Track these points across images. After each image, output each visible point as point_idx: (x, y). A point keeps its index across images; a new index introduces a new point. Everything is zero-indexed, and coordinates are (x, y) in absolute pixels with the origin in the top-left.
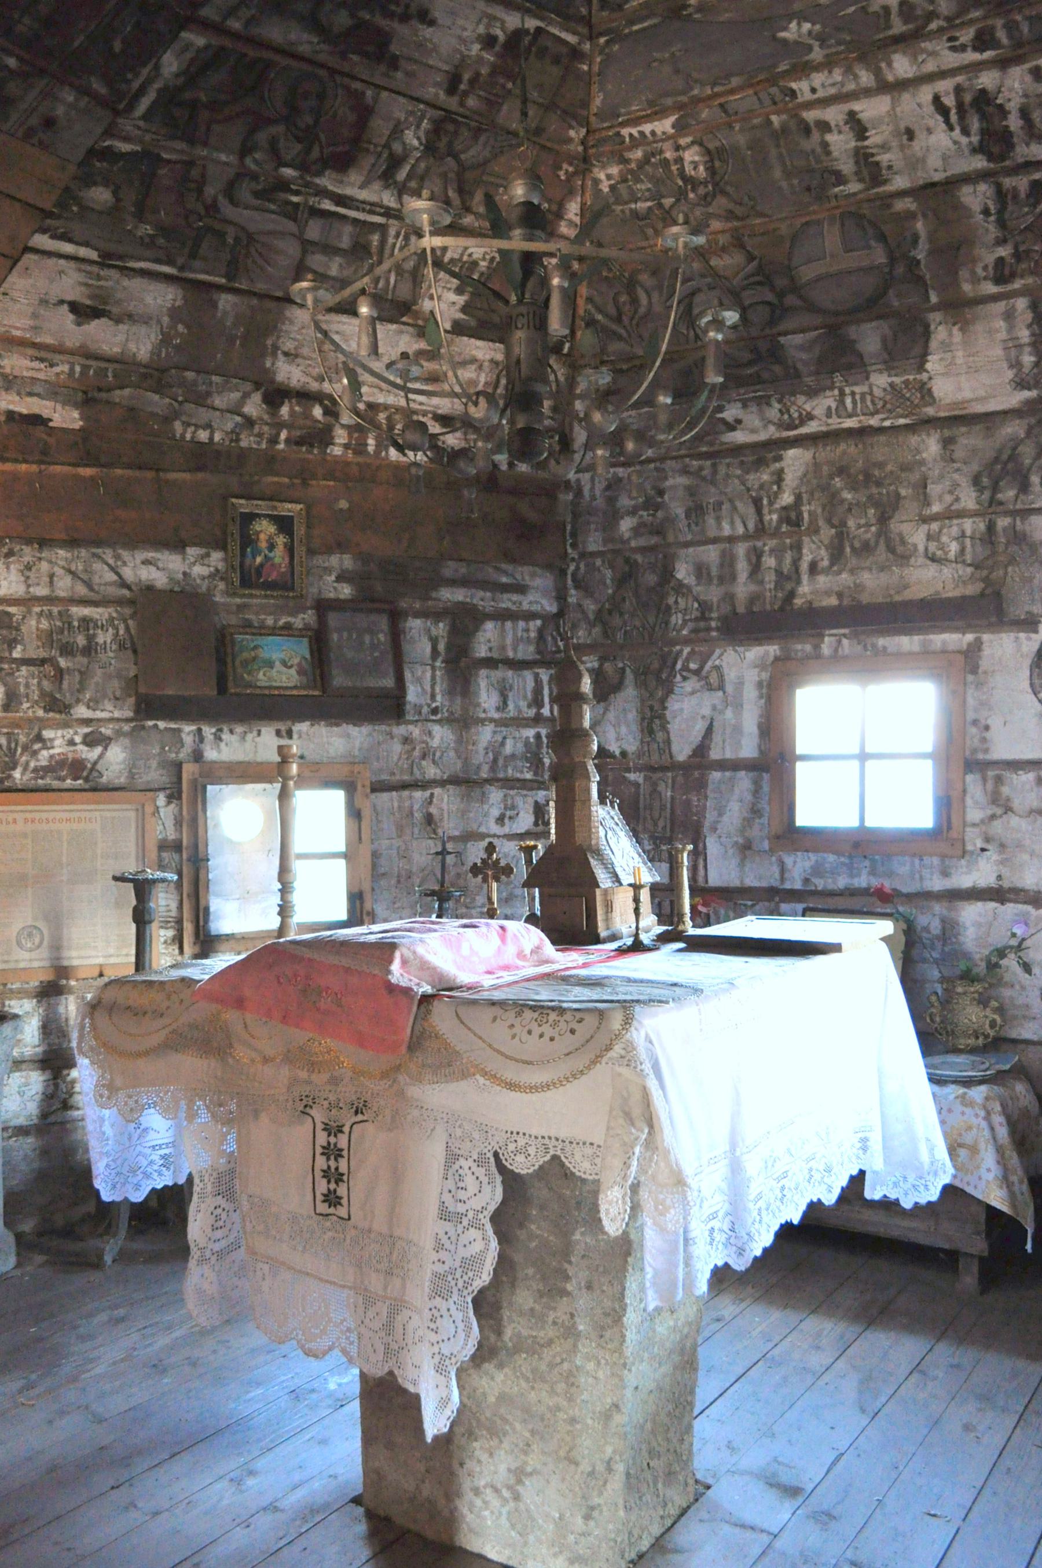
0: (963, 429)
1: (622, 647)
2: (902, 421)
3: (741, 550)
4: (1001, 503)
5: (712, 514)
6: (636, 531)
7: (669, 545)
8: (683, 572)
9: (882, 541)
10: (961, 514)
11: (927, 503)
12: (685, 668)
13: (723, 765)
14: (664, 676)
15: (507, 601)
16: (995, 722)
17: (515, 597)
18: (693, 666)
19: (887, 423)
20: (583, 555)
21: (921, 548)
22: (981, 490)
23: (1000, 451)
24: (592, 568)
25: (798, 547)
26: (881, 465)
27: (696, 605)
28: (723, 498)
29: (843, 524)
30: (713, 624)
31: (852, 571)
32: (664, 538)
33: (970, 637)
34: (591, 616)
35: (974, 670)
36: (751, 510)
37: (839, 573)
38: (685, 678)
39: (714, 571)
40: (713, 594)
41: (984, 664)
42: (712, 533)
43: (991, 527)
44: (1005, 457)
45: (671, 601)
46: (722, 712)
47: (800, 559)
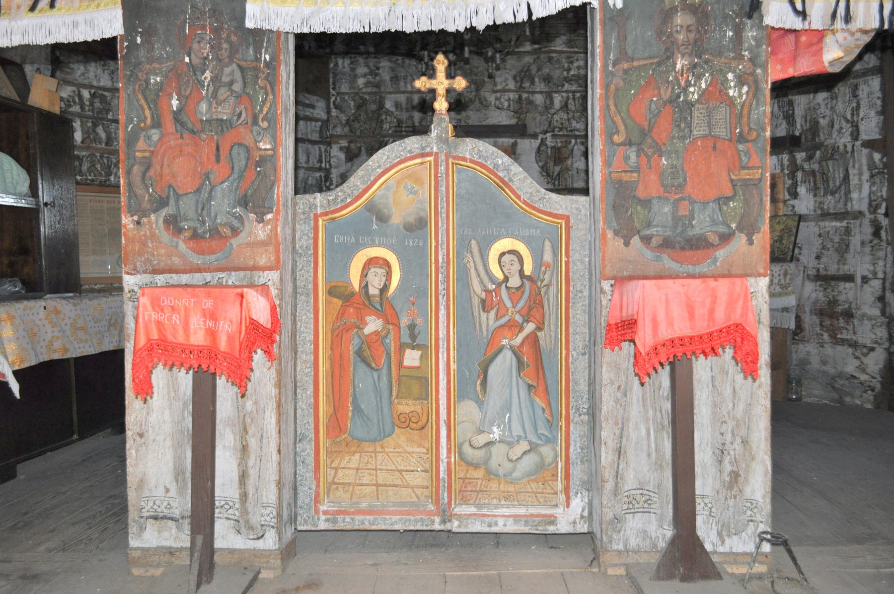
1: (359, 137)
6: (367, 84)
8: (389, 105)
10: (509, 91)
11: (495, 85)
15: (308, 112)
17: (311, 110)
20: (338, 94)
22: (516, 82)
24: (343, 100)
26: (477, 67)
34: (344, 122)
39: (404, 106)
40: (404, 116)
42: (402, 89)
43: (520, 97)
45: (383, 117)
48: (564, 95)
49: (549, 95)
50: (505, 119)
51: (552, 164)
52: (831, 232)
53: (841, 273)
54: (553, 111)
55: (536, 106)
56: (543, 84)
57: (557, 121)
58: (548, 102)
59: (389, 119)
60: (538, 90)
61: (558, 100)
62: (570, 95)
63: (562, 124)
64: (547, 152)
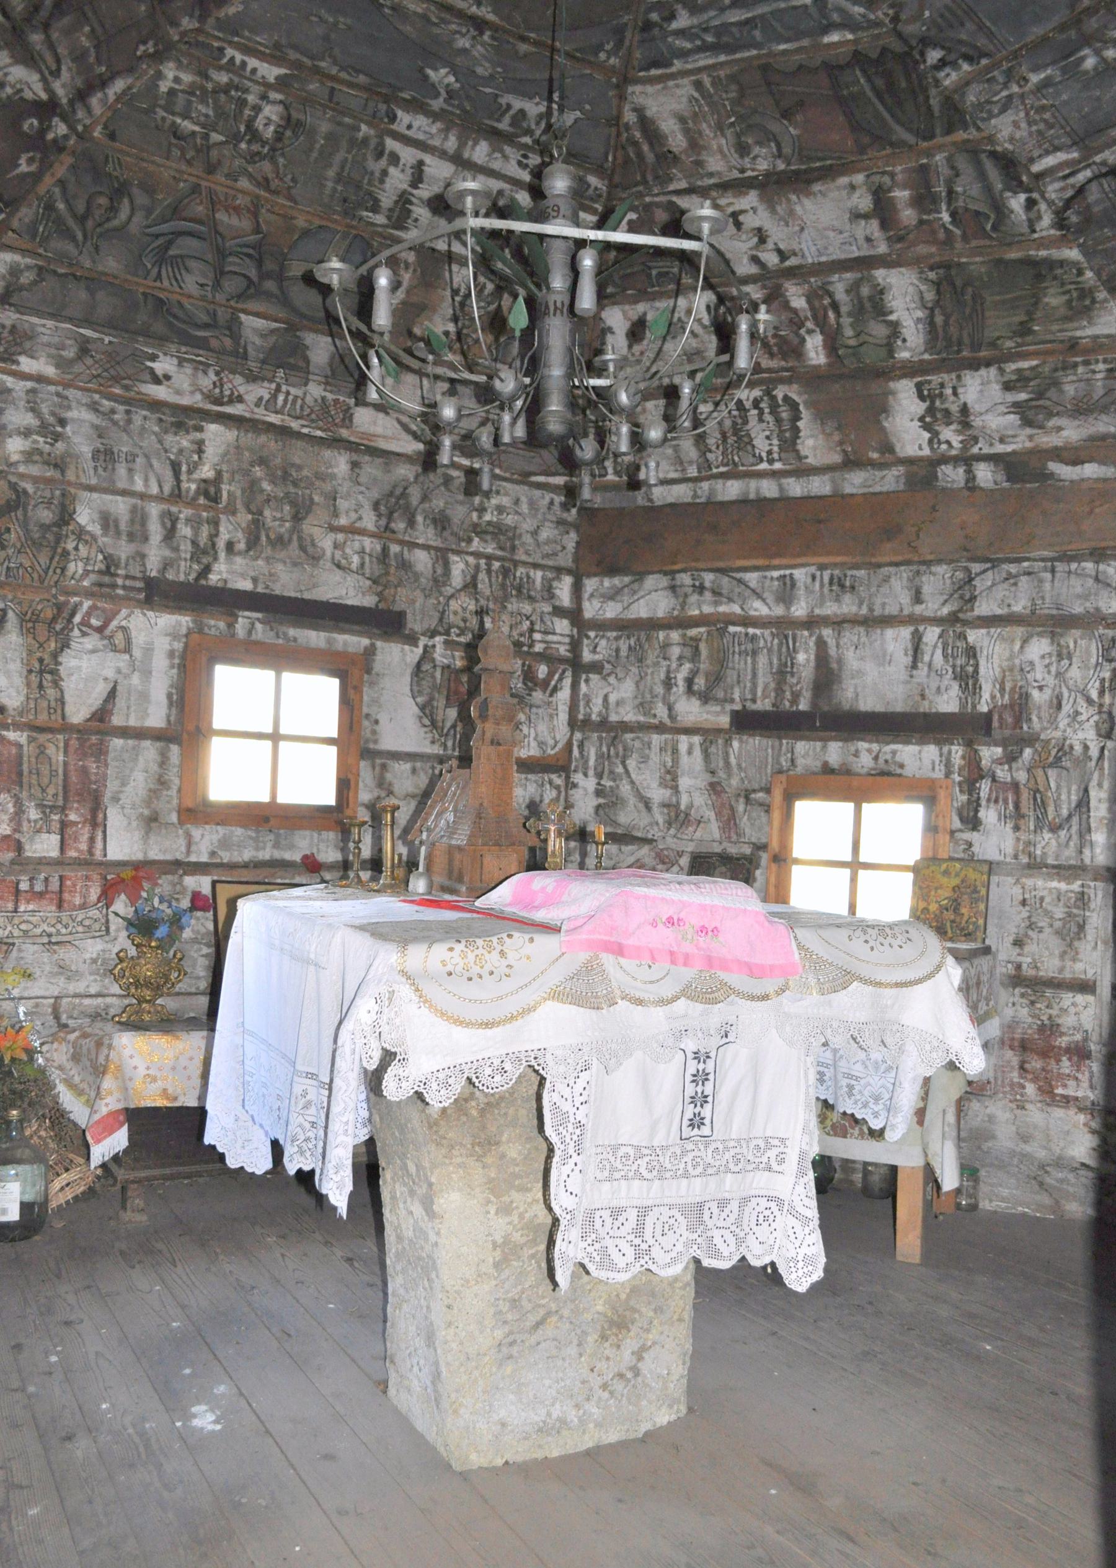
0: (367, 458)
2: (319, 433)
3: (154, 510)
4: (394, 532)
5: (124, 464)
7: (69, 483)
8: (84, 517)
9: (295, 537)
10: (362, 532)
11: (336, 514)
12: (85, 623)
13: (125, 732)
14: (58, 627)
16: (383, 718)
18: (94, 622)
19: (305, 431)
21: (328, 553)
22: (379, 516)
23: (394, 487)
25: (216, 523)
26: (299, 468)
27: (100, 557)
28: (137, 451)
29: (261, 513)
30: (120, 582)
31: (267, 559)
32: (63, 472)
33: (366, 642)
35: (369, 671)
36: (168, 474)
37: (256, 559)
38: (84, 634)
39: (123, 526)
40: (123, 550)
41: (377, 667)
42: (121, 485)
43: (385, 550)
44: (398, 492)
45: (70, 546)
46: (127, 677)
47: (217, 535)
48: (471, 560)
49: (442, 556)
50: (352, 593)
51: (440, 702)
52: (1047, 900)
53: (1068, 975)
54: (449, 591)
55: (417, 576)
56: (431, 531)
57: (455, 613)
58: (439, 571)
59: (83, 551)
60: (420, 541)
61: (458, 568)
62: (483, 562)
63: (465, 620)
64: (433, 677)
